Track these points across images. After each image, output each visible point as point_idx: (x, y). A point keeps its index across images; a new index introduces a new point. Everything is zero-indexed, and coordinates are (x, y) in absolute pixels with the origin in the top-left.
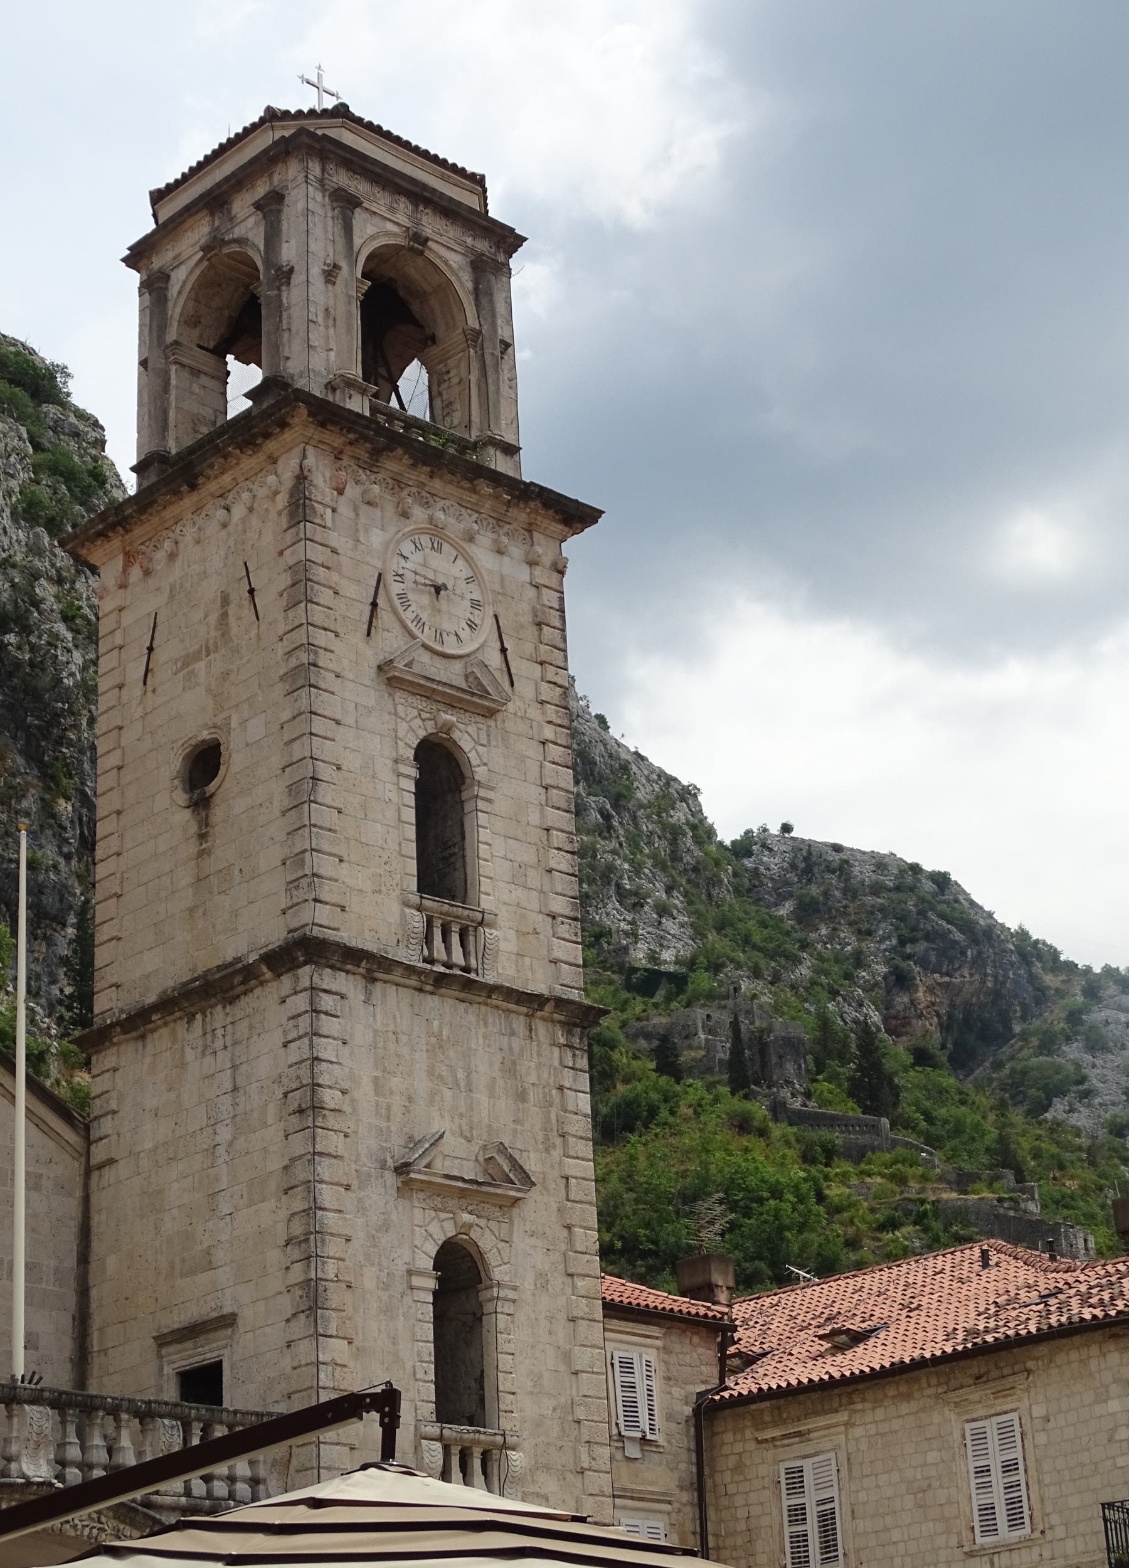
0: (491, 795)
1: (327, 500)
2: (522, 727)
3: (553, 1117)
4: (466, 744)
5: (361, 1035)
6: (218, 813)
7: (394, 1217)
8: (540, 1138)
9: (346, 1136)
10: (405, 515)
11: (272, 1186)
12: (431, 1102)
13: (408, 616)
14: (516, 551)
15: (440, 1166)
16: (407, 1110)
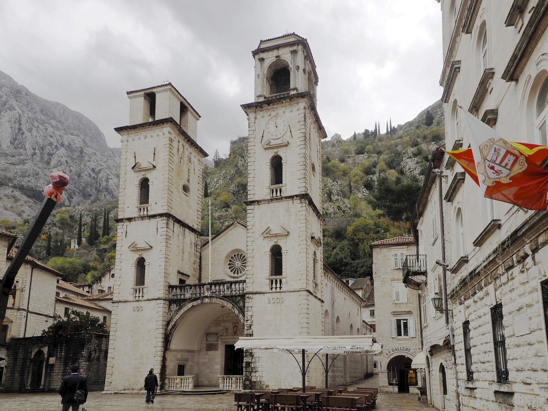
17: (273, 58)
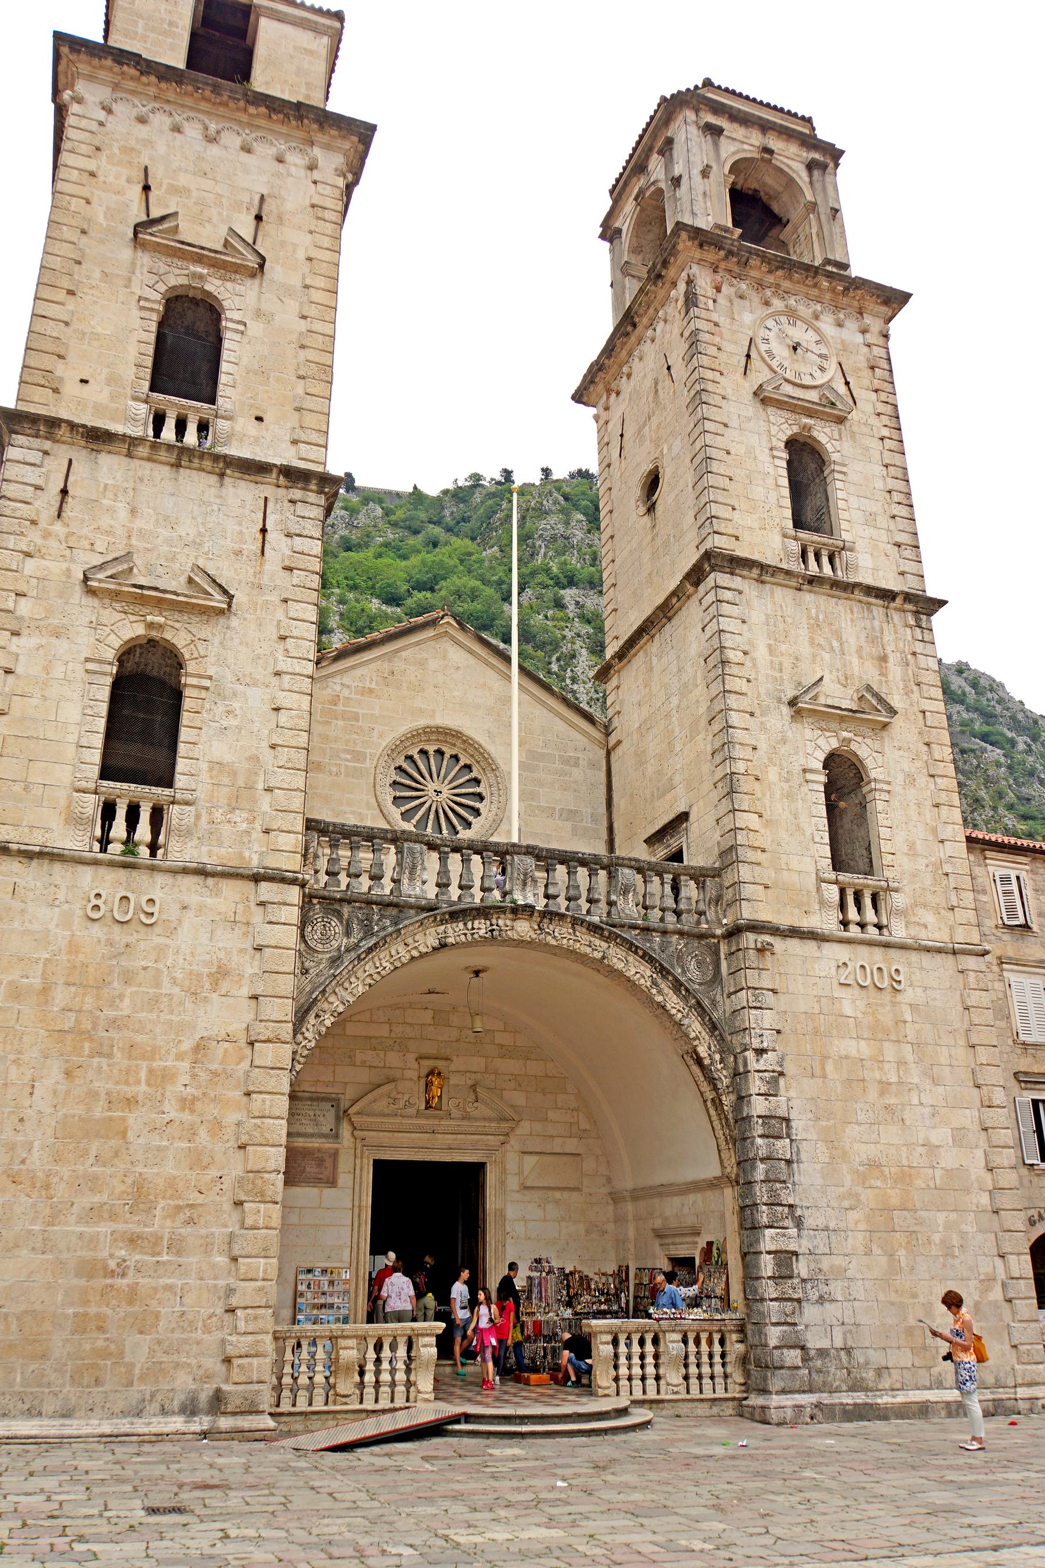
0: (844, 469)
1: (709, 294)
2: (865, 430)
3: (910, 673)
4: (822, 438)
5: (756, 617)
6: (659, 507)
7: (790, 734)
8: (901, 686)
9: (749, 681)
10: (767, 303)
11: (703, 722)
12: (814, 662)
13: (774, 364)
14: (852, 325)
15: (822, 700)
16: (794, 666)
17: (746, 147)
